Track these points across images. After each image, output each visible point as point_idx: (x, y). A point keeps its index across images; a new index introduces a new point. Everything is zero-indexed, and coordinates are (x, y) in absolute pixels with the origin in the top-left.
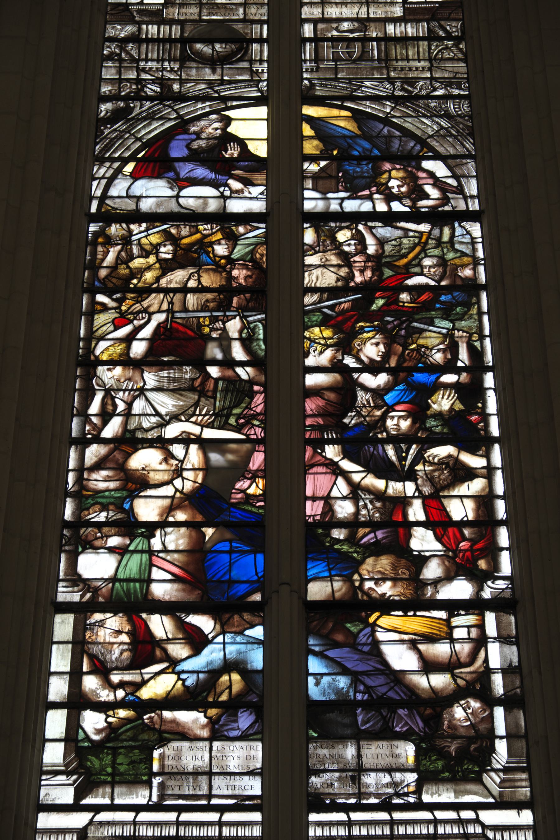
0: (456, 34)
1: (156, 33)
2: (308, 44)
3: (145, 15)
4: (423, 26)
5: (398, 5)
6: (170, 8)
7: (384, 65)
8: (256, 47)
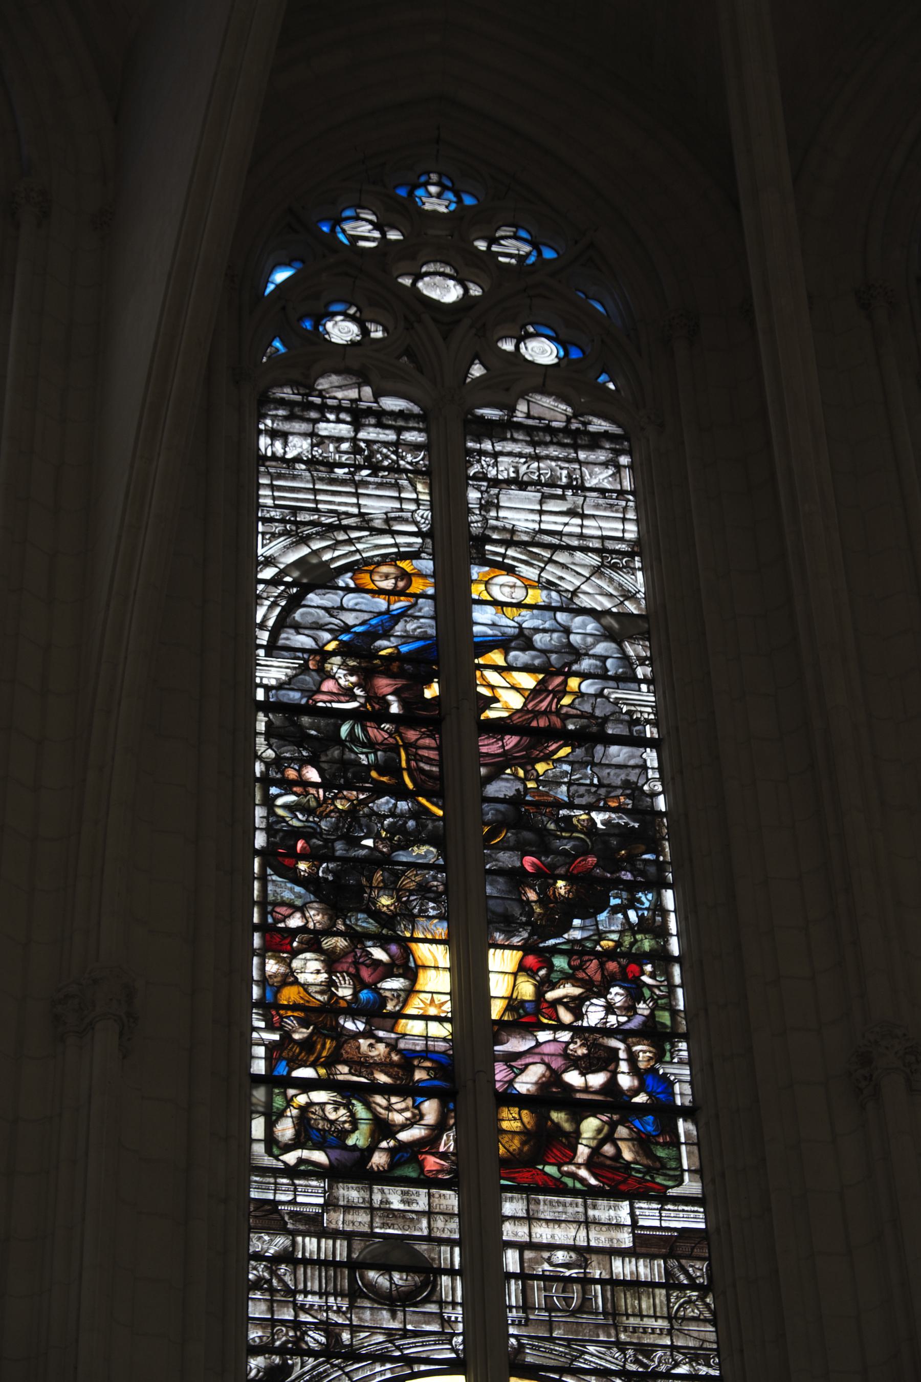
0: (702, 1280)
1: (315, 1249)
2: (513, 1282)
3: (299, 1221)
4: (659, 1265)
5: (626, 1229)
6: (332, 1212)
7: (611, 1322)
8: (445, 1280)
